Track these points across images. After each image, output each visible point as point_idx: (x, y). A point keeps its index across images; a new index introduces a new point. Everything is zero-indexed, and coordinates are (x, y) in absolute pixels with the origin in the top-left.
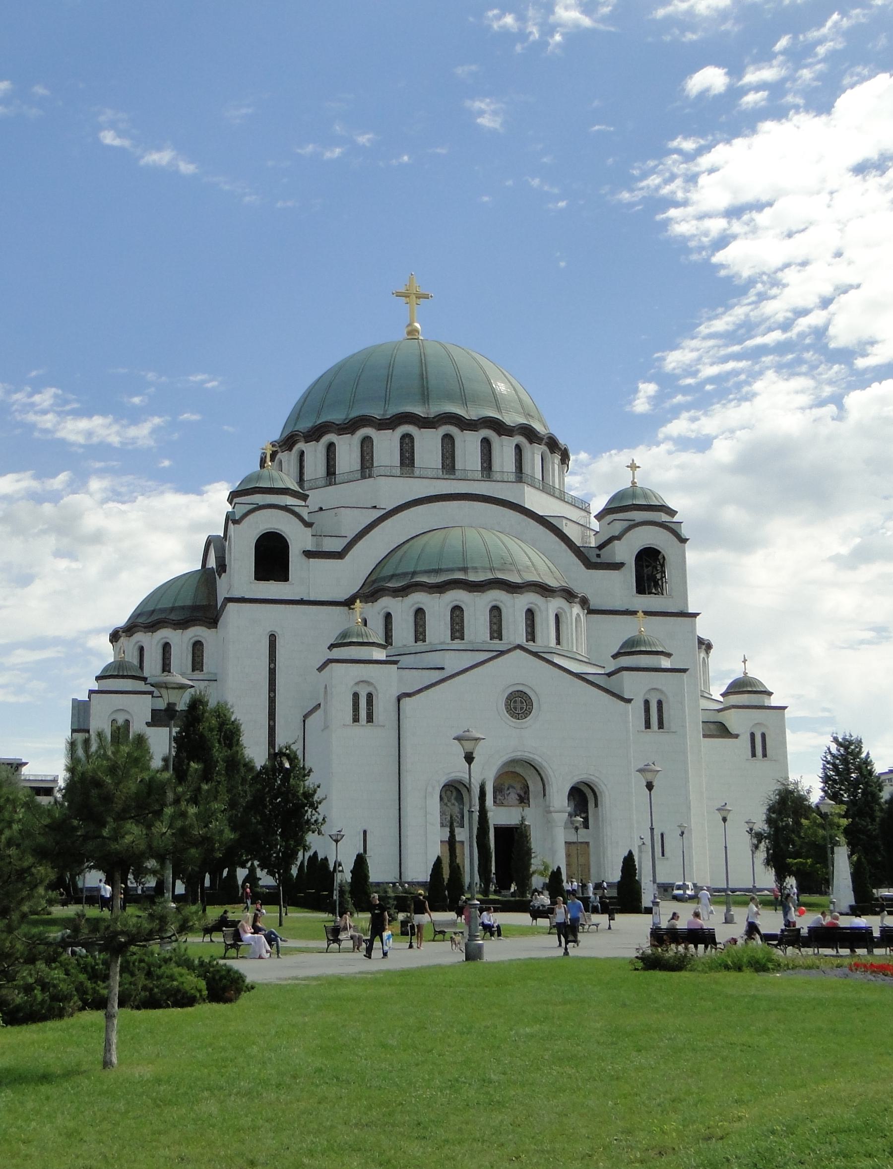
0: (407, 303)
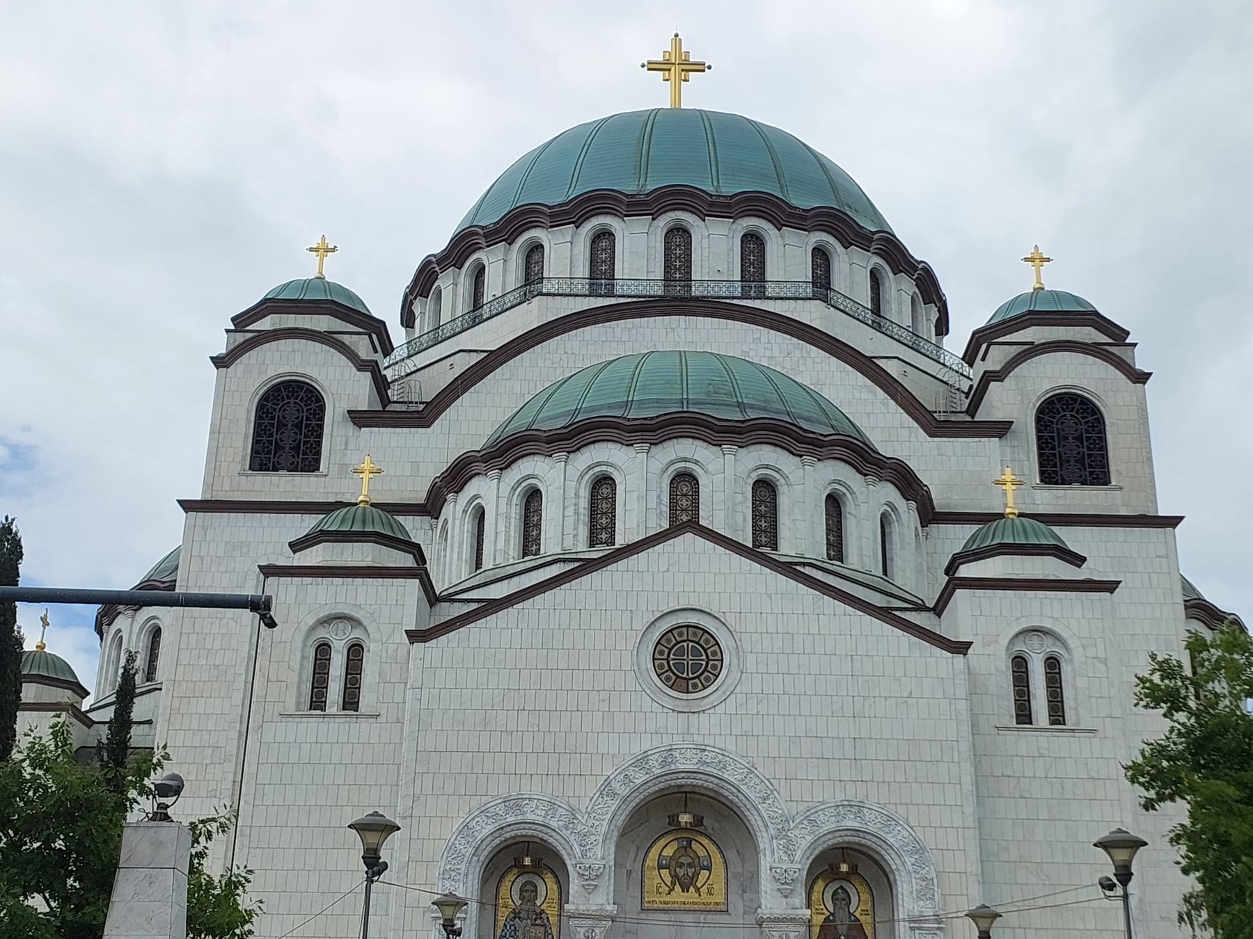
0: (667, 80)
